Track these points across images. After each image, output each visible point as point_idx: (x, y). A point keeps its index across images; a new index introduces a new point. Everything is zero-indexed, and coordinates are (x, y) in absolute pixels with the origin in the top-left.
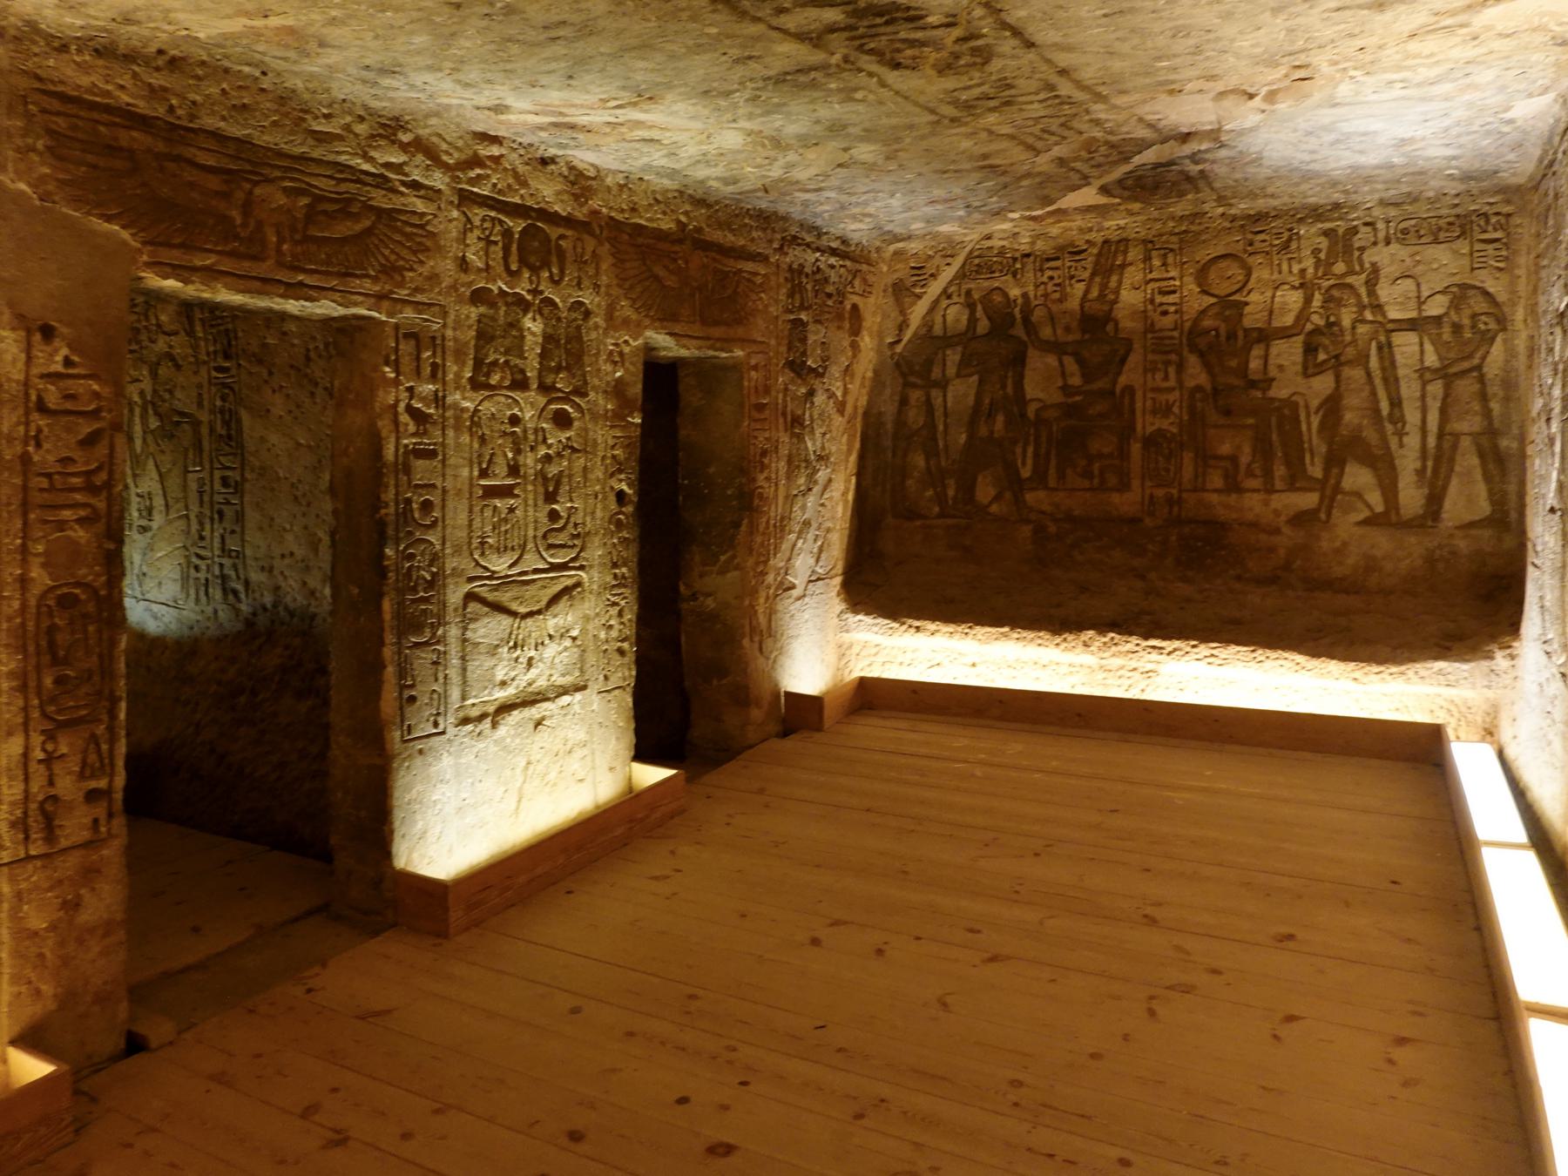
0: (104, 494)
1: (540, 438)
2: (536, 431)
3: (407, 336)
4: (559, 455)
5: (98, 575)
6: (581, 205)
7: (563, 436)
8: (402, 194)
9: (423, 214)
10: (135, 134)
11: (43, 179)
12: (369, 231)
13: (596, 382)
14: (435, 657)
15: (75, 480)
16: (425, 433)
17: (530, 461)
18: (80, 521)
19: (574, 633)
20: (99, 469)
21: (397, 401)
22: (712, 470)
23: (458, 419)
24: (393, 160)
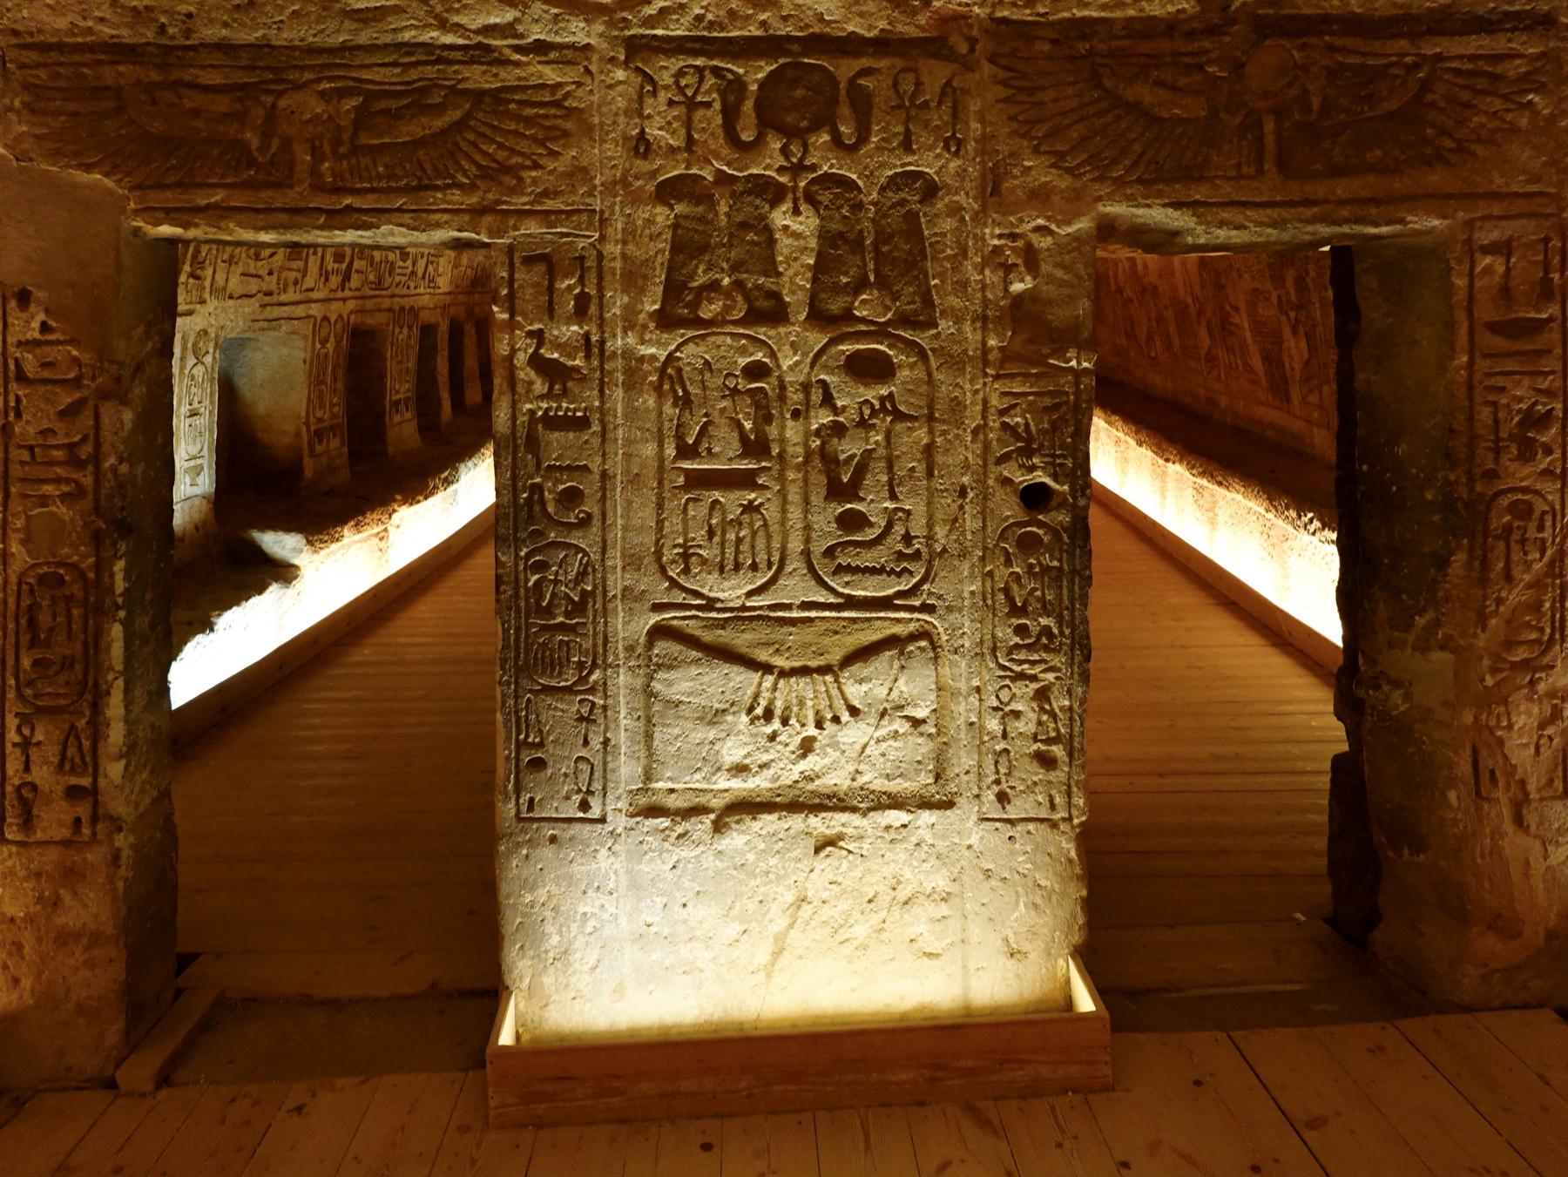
0: (90, 468)
1: (816, 396)
2: (806, 387)
3: (529, 261)
4: (863, 424)
5: (85, 557)
6: (914, 12)
7: (874, 393)
8: (517, 64)
9: (559, 85)
10: (121, 68)
11: (20, 138)
12: (459, 126)
13: (954, 301)
14: (585, 711)
15: (55, 453)
16: (565, 392)
17: (793, 432)
18: (64, 497)
19: (920, 713)
20: (84, 440)
21: (514, 351)
22: (1402, 449)
23: (630, 372)
24: (493, 20)
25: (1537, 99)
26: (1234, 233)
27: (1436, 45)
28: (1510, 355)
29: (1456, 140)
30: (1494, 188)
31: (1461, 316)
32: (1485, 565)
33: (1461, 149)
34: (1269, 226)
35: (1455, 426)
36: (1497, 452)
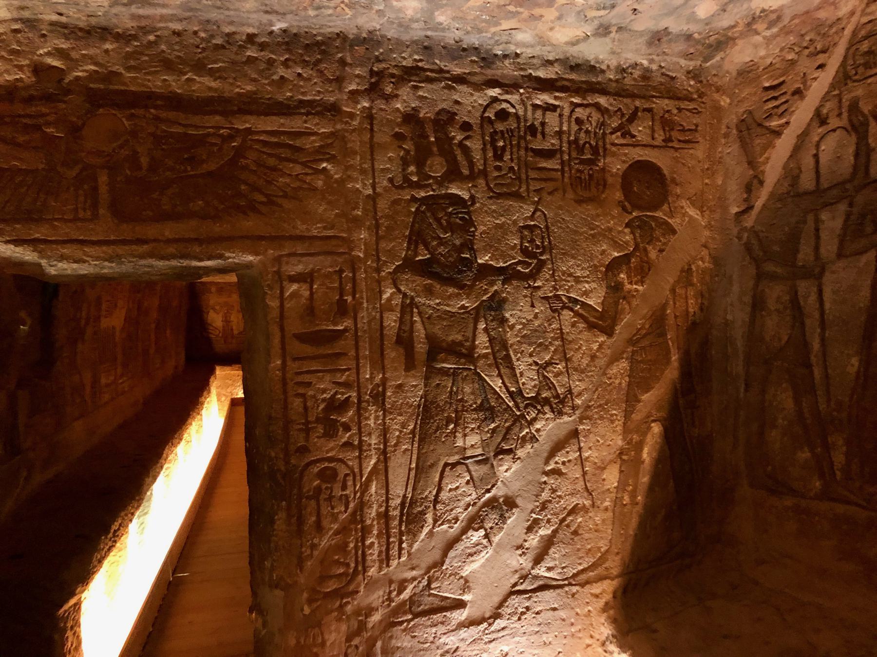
25: (329, 167)
26: (75, 266)
27: (245, 122)
28: (314, 358)
29: (266, 196)
30: (298, 232)
31: (275, 330)
32: (301, 521)
33: (271, 202)
34: (106, 260)
35: (273, 415)
36: (307, 431)
